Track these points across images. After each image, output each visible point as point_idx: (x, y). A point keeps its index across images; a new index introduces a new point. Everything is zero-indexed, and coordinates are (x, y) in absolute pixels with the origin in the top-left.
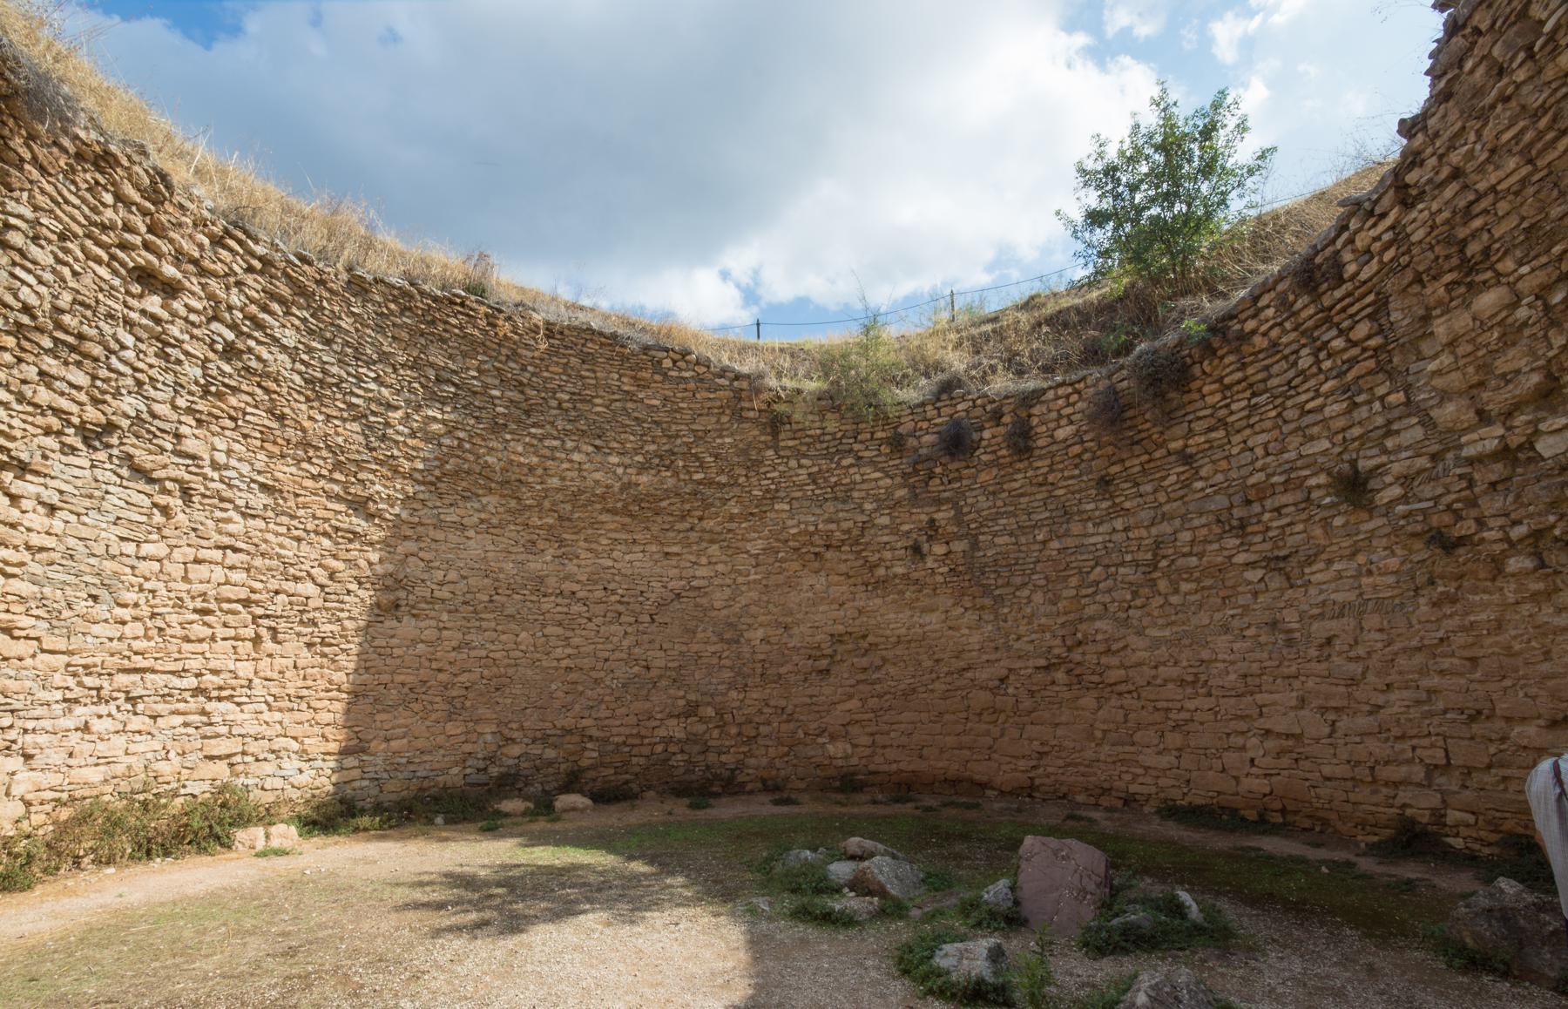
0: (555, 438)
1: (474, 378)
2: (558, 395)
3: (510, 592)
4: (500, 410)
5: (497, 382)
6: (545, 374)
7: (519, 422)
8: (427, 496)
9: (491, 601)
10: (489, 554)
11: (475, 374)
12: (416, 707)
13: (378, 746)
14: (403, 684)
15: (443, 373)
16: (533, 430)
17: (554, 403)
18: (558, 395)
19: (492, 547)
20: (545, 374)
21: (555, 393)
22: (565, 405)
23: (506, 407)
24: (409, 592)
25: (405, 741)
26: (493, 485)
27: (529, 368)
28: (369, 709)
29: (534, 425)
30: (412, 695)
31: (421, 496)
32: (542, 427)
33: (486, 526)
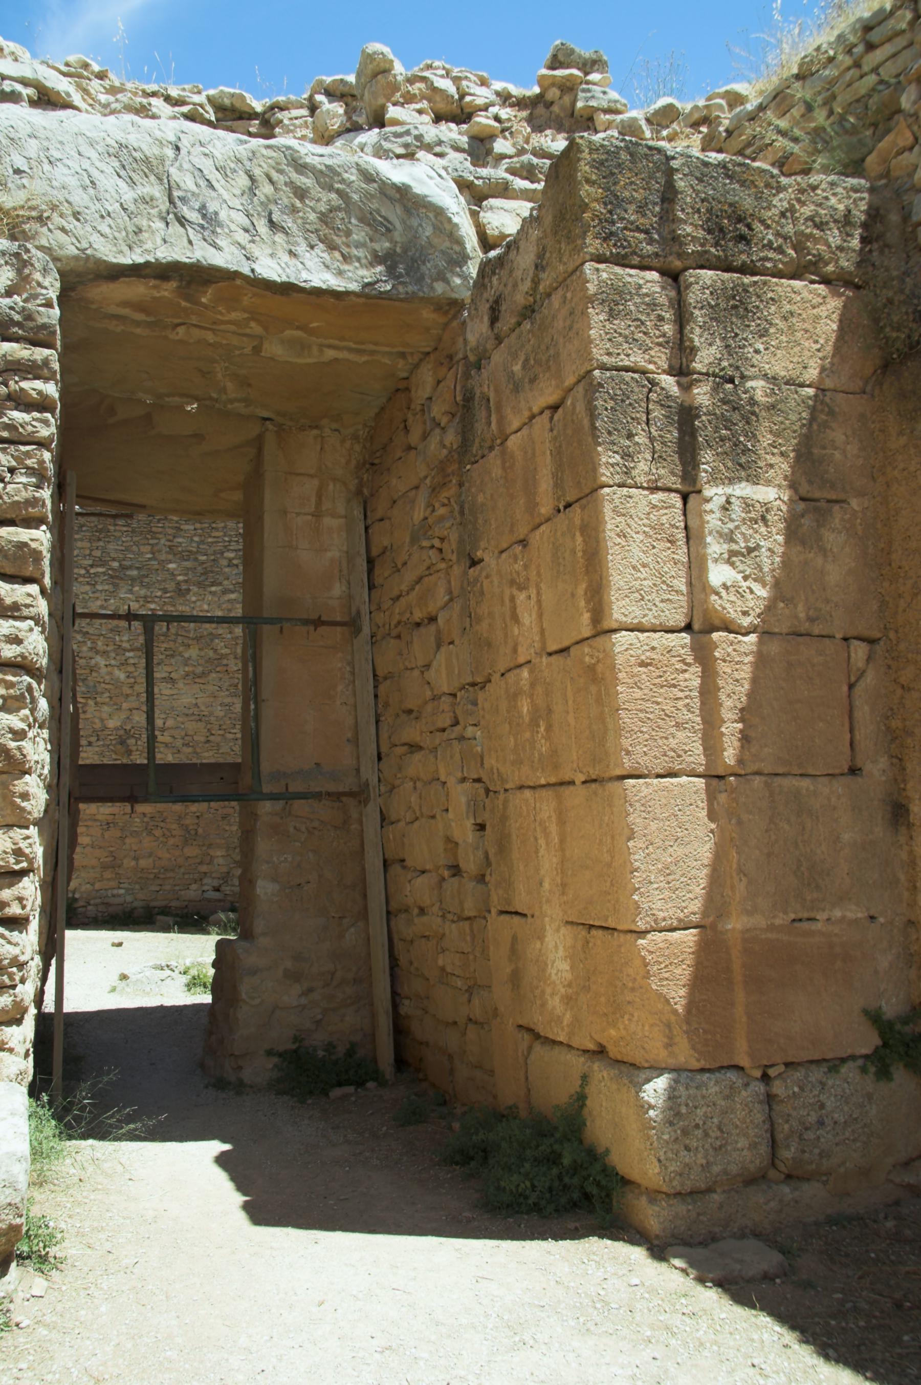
0: (233, 592)
1: (150, 559)
2: (226, 555)
3: (221, 732)
4: (180, 578)
5: (170, 557)
6: (210, 540)
7: (200, 584)
8: (135, 661)
9: (208, 741)
10: (199, 701)
11: (149, 556)
12: (158, 833)
13: (129, 863)
14: (144, 814)
15: (124, 563)
16: (213, 589)
17: (225, 562)
18: (226, 555)
19: (201, 695)
20: (210, 540)
21: (222, 553)
22: (235, 562)
23: (186, 575)
24: (137, 739)
25: (151, 860)
26: (190, 642)
27: (196, 539)
28: (119, 834)
29: (213, 584)
30: (152, 823)
31: (132, 661)
32: (220, 584)
33: (194, 677)
